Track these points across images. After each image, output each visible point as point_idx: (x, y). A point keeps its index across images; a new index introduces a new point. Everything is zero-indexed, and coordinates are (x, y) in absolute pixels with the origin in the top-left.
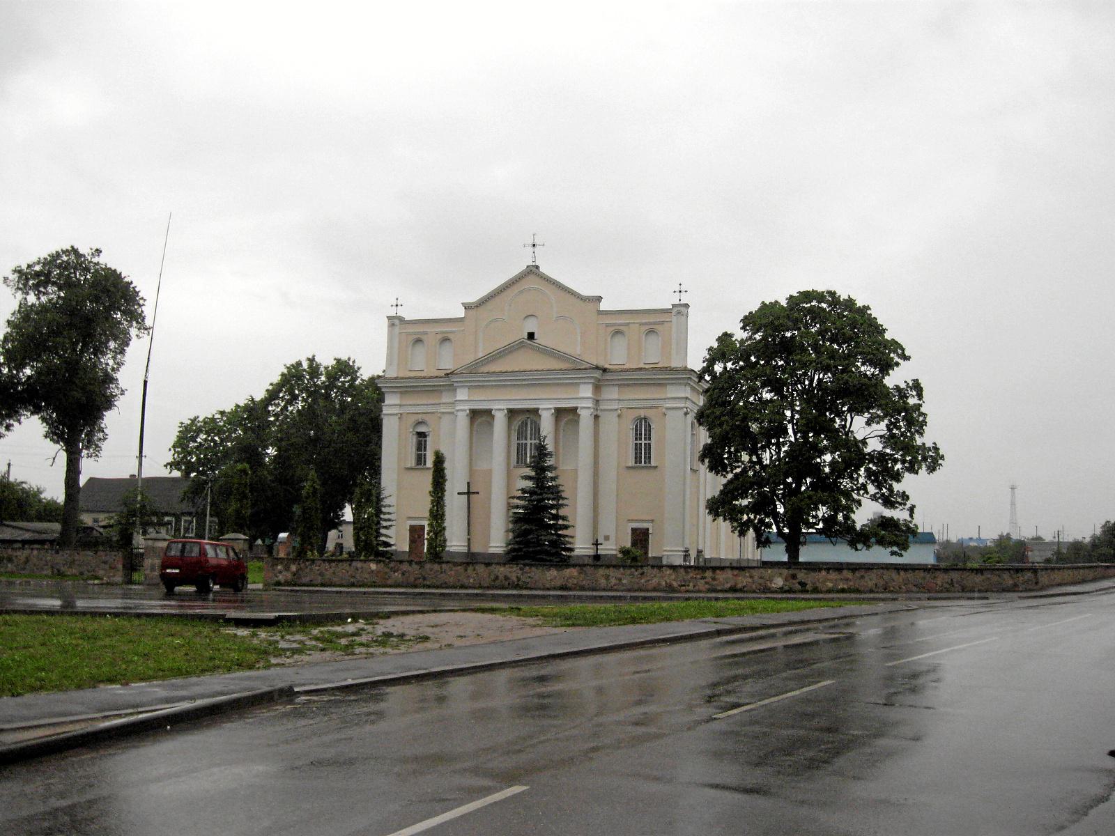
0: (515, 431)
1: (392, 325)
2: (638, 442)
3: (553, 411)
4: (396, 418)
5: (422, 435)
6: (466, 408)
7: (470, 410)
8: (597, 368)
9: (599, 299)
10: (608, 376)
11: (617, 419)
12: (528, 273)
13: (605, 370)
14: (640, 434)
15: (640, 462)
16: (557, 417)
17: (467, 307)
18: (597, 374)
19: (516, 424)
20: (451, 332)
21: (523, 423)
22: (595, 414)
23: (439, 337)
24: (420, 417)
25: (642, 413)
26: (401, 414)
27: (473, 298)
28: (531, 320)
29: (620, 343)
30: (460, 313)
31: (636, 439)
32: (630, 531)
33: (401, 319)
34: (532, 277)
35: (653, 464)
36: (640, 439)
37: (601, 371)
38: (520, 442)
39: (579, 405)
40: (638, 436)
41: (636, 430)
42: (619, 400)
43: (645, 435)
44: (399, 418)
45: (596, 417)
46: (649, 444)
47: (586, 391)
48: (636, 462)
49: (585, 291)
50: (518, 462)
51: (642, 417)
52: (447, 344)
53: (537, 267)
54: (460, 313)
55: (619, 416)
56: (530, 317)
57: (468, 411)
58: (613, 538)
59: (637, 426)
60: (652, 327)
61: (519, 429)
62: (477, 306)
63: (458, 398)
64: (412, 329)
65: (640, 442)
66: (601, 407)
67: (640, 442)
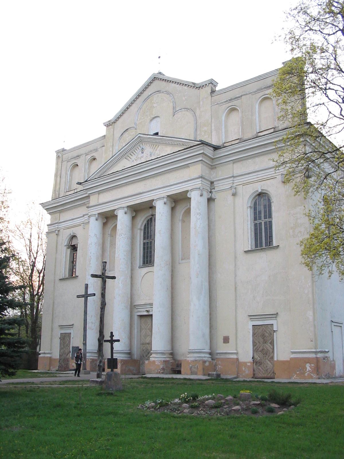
0: (141, 229)
1: (58, 157)
2: (258, 222)
3: (165, 200)
4: (54, 235)
5: (74, 248)
6: (94, 213)
7: (99, 214)
8: (203, 143)
9: (212, 83)
10: (221, 153)
11: (230, 198)
12: (153, 80)
13: (216, 148)
14: (260, 212)
15: (261, 246)
16: (173, 209)
17: (109, 124)
18: (209, 151)
19: (141, 221)
20: (96, 150)
21: (148, 221)
22: (209, 197)
23: (89, 157)
24: (70, 232)
25: (259, 187)
26: (59, 231)
27: (111, 116)
28: (154, 121)
29: (235, 117)
30: (103, 131)
31: (255, 219)
32: (251, 327)
33: (63, 150)
34: (156, 82)
35: (275, 244)
36: (260, 219)
37: (212, 149)
38: (146, 241)
39: (189, 188)
40: (256, 216)
41: (255, 209)
42: (233, 177)
43: (265, 212)
44: (57, 235)
45: (210, 200)
46: (271, 222)
47: (197, 170)
48: (256, 246)
49: (198, 80)
50: (144, 263)
51: (260, 191)
52: (95, 162)
53: (160, 73)
54: (103, 131)
55: (234, 195)
56: (156, 119)
57: (97, 216)
58: (232, 340)
59: (255, 204)
60: (261, 94)
61: (145, 228)
62: (114, 123)
63: (91, 204)
64: (70, 155)
65: (260, 221)
66: (216, 189)
67: (260, 221)
